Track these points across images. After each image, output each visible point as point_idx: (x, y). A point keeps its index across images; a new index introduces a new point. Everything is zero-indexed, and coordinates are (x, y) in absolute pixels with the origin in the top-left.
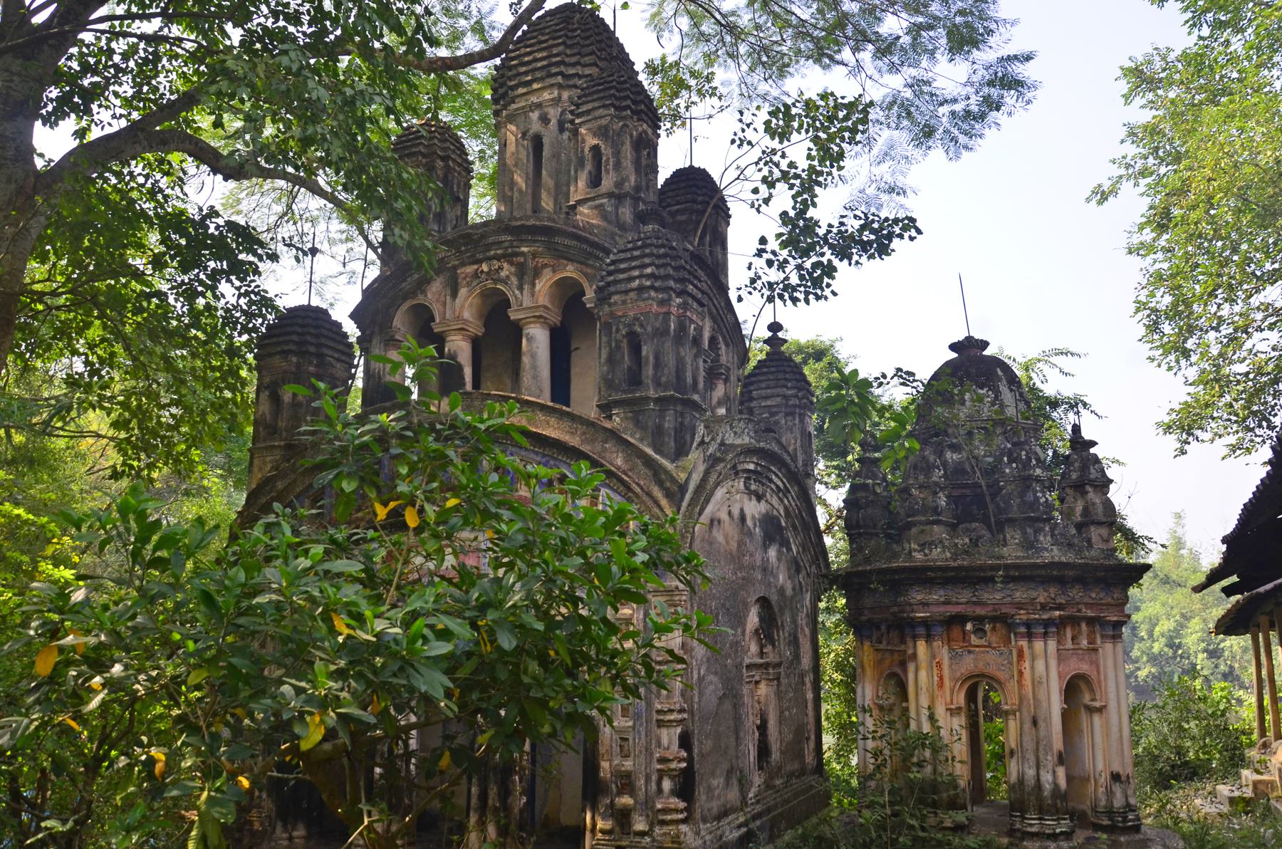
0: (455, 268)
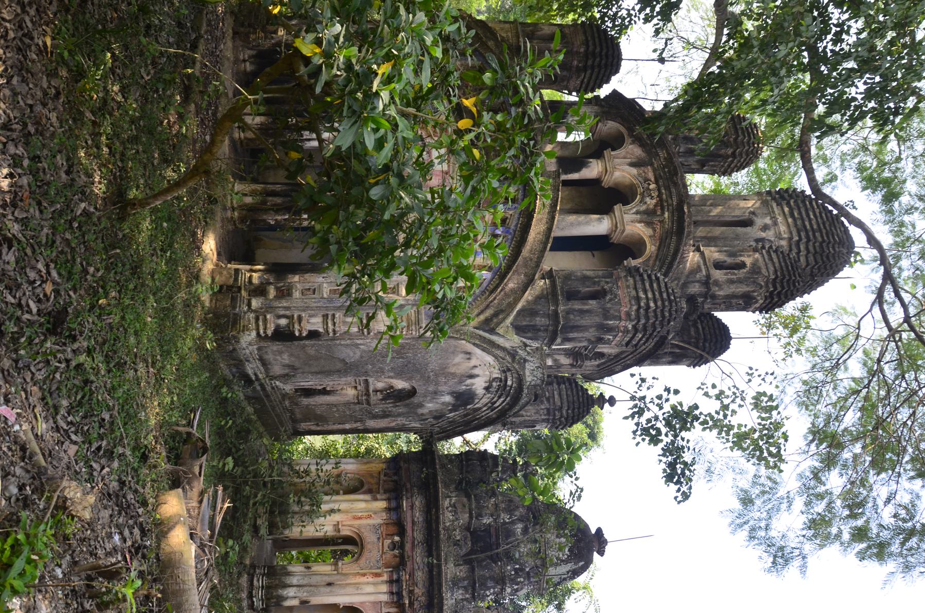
0: (652, 165)
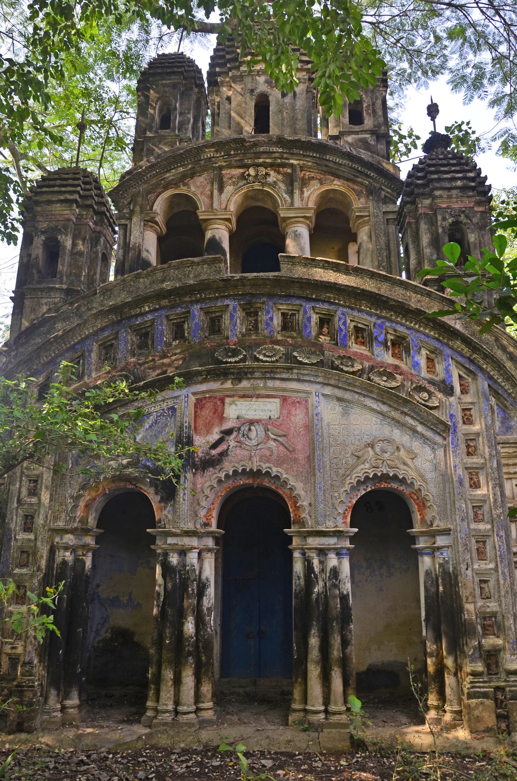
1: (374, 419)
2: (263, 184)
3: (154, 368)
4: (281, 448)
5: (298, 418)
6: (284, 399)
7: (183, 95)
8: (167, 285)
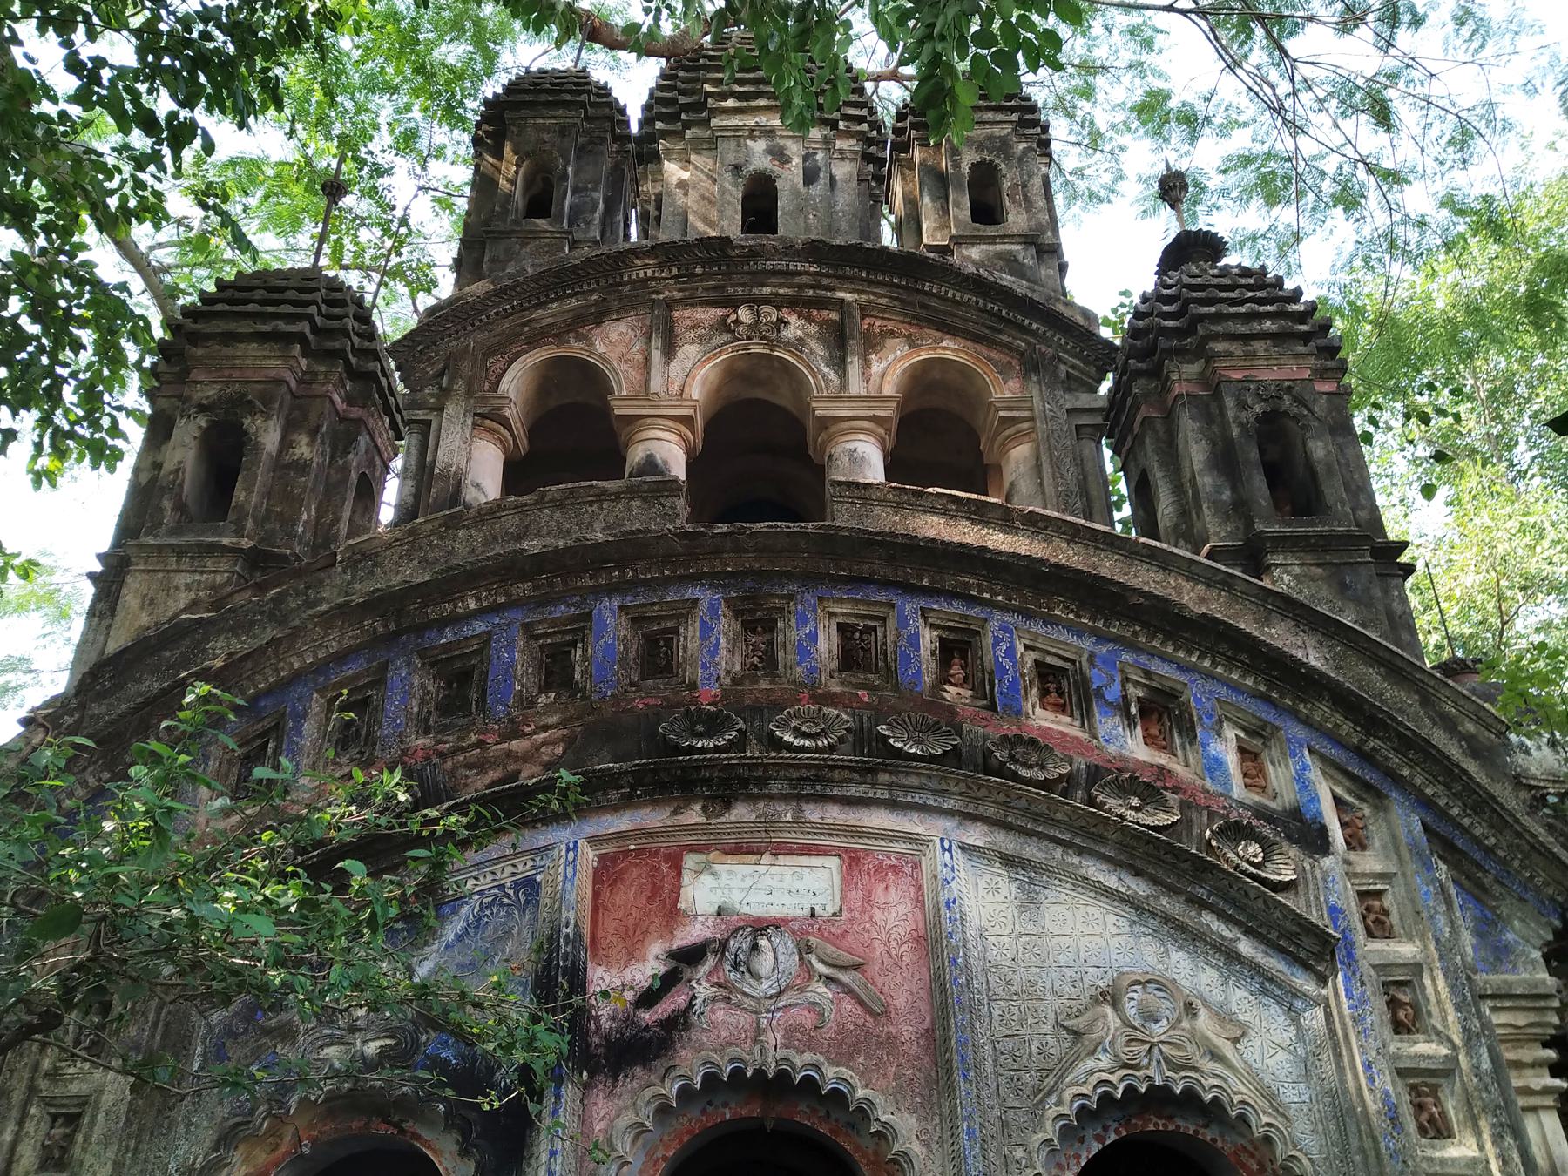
0: (670, 304)
1: (1112, 918)
2: (772, 344)
3: (481, 766)
4: (848, 1006)
5: (894, 914)
6: (853, 860)
7: (582, 151)
8: (533, 545)
